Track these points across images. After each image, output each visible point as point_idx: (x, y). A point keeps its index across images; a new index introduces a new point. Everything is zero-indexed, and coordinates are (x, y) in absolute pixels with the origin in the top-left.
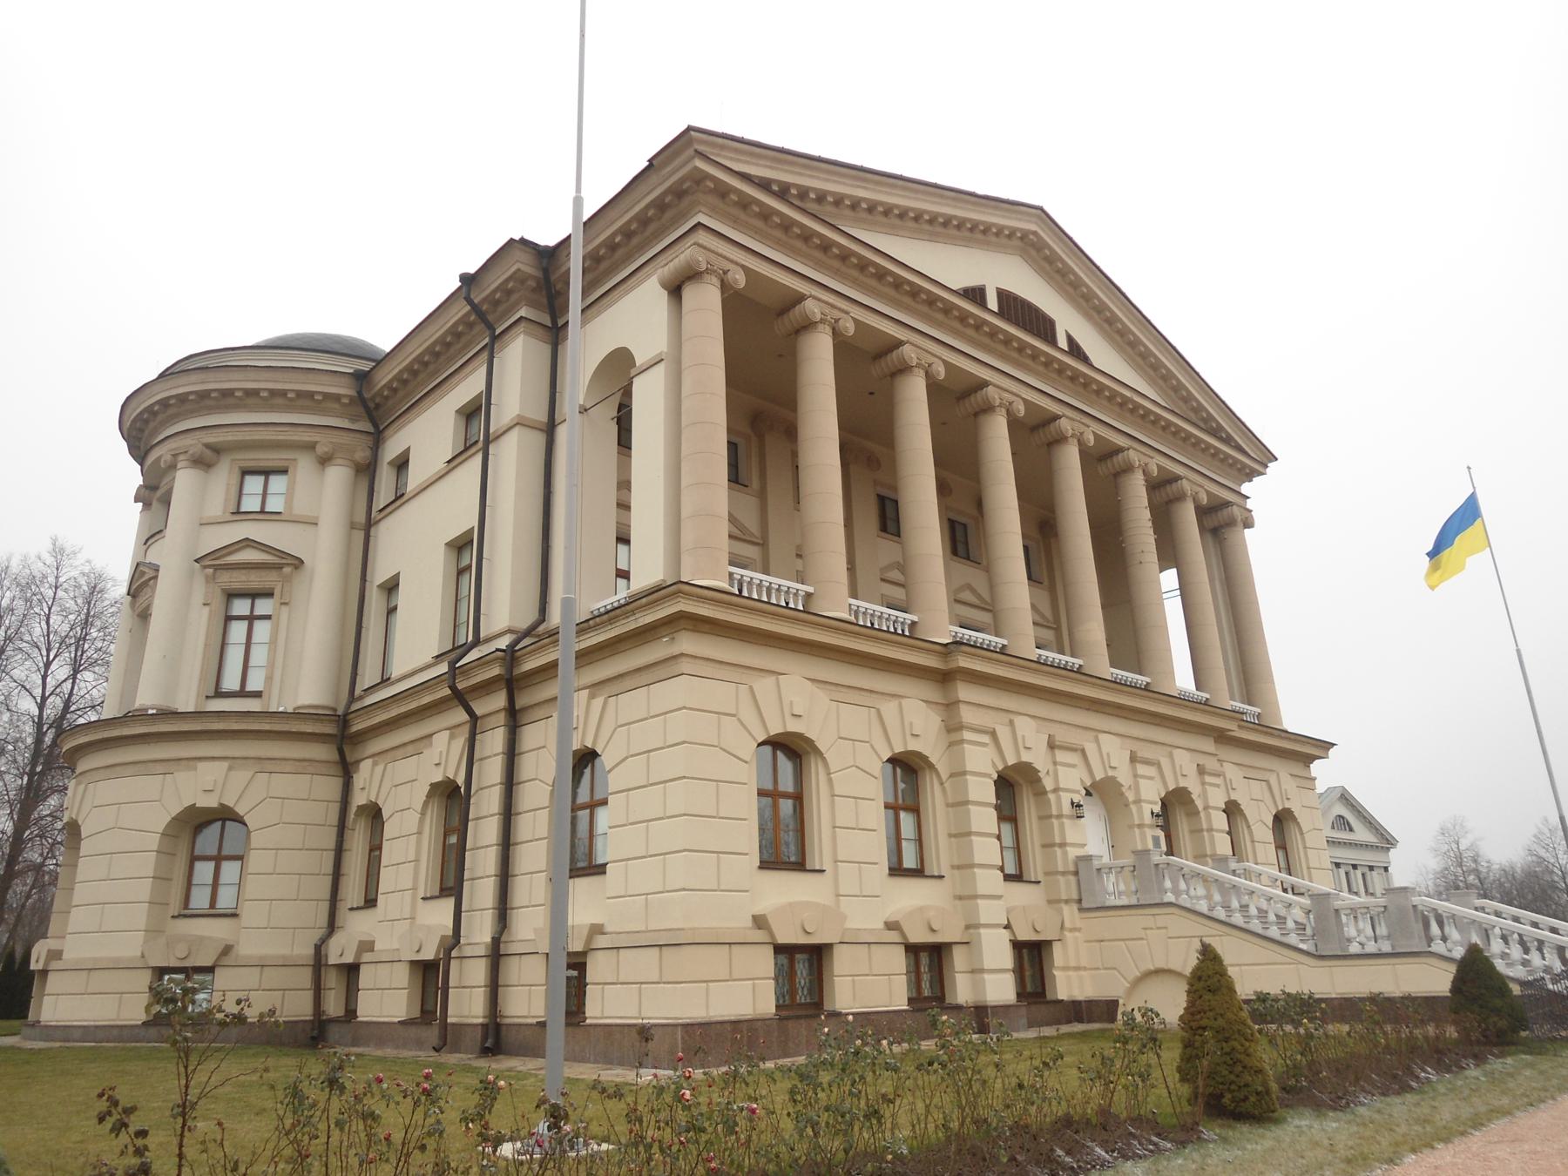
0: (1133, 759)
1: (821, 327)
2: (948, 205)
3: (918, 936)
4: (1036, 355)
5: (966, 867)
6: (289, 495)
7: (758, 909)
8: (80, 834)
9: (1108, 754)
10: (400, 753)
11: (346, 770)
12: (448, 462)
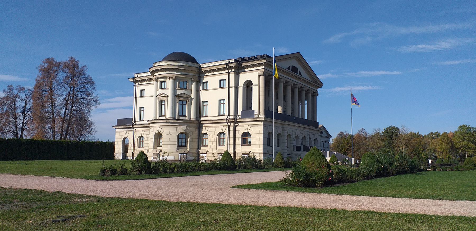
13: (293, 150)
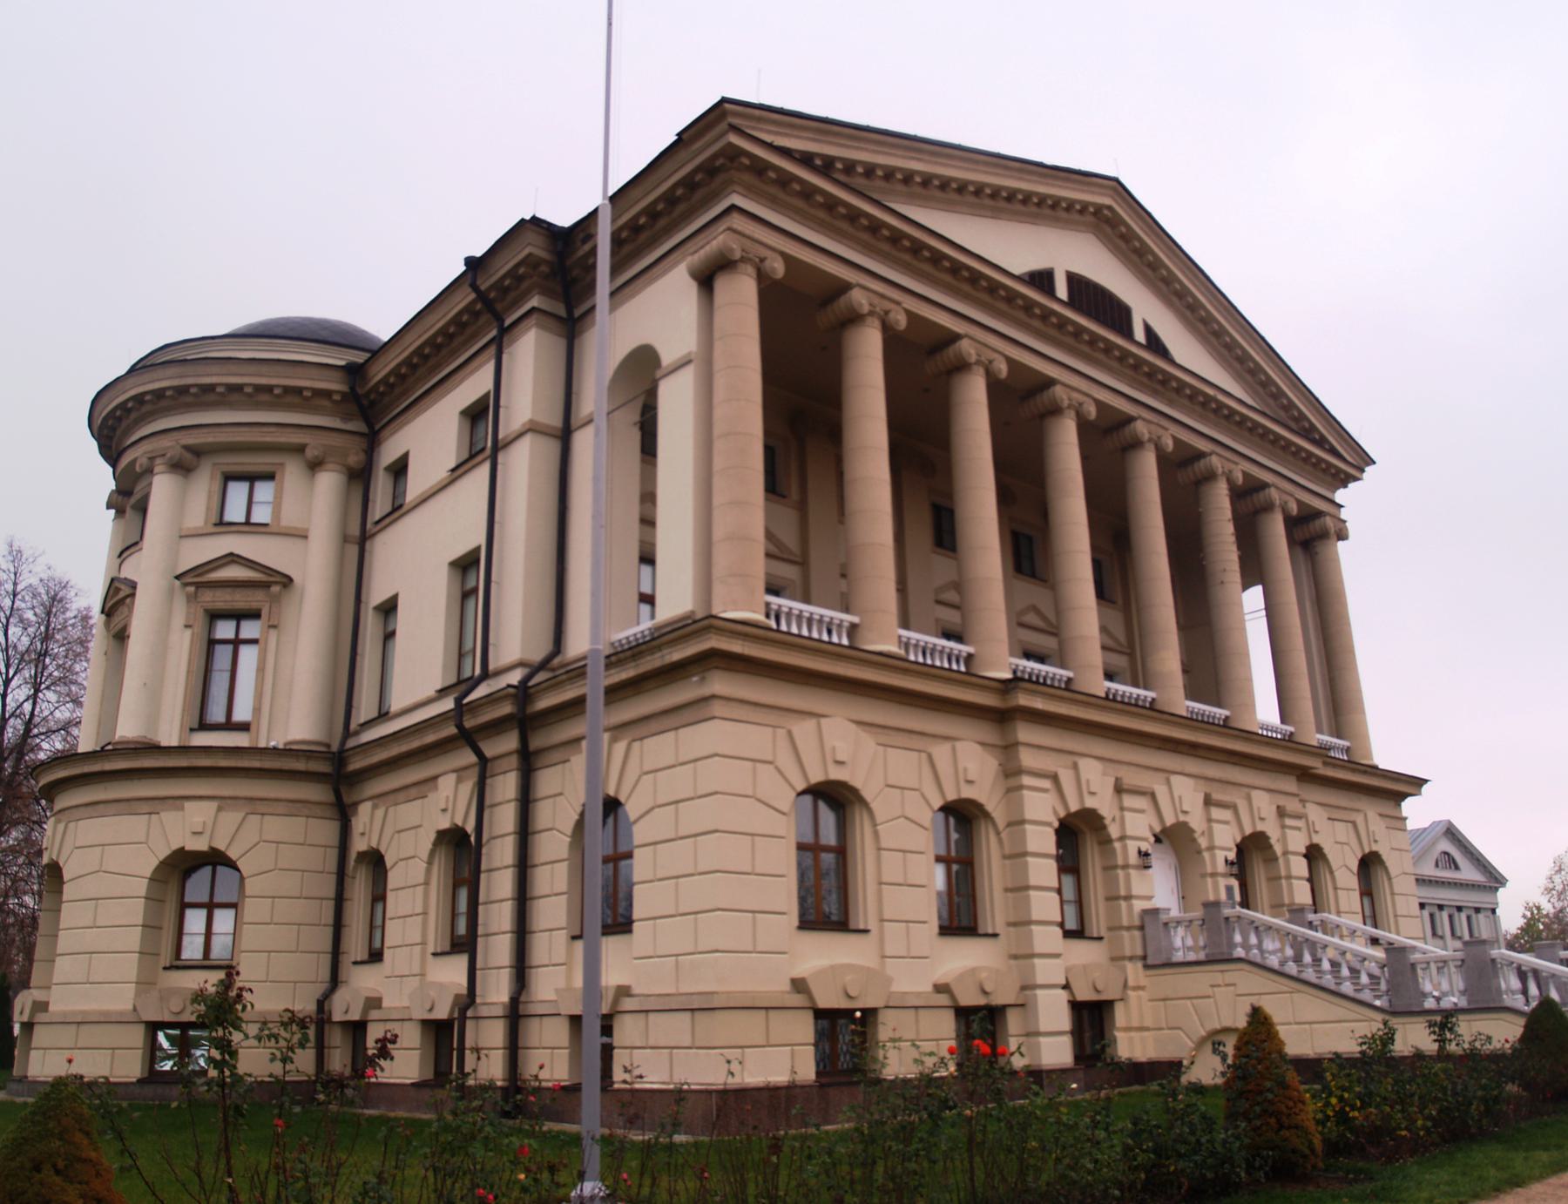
0: (1208, 802)
1: (869, 320)
2: (1011, 177)
3: (969, 998)
4: (1109, 348)
5: (1022, 923)
7: (798, 972)
8: (61, 877)
9: (1180, 798)
10: (401, 796)
11: (344, 814)
12: (453, 470)
13: (1144, 958)
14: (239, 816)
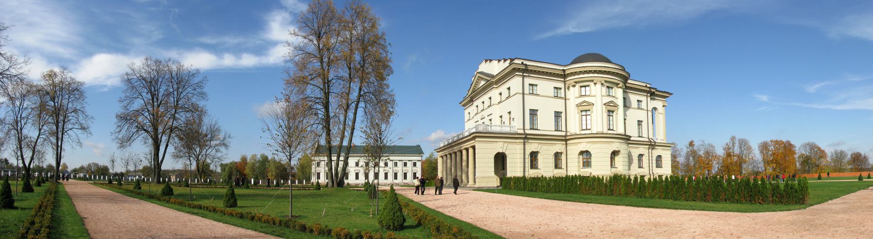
6: (590, 91)
14: (590, 145)
